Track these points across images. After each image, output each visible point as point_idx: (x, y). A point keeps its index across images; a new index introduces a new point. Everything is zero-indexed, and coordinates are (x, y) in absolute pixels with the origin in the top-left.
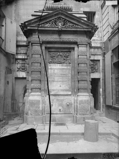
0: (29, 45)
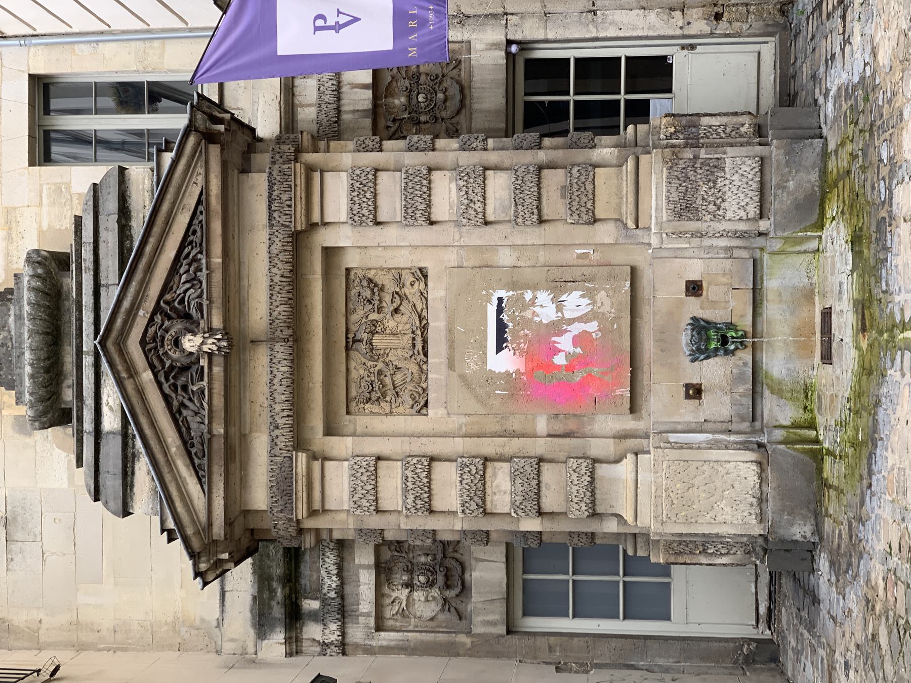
0: (318, 531)
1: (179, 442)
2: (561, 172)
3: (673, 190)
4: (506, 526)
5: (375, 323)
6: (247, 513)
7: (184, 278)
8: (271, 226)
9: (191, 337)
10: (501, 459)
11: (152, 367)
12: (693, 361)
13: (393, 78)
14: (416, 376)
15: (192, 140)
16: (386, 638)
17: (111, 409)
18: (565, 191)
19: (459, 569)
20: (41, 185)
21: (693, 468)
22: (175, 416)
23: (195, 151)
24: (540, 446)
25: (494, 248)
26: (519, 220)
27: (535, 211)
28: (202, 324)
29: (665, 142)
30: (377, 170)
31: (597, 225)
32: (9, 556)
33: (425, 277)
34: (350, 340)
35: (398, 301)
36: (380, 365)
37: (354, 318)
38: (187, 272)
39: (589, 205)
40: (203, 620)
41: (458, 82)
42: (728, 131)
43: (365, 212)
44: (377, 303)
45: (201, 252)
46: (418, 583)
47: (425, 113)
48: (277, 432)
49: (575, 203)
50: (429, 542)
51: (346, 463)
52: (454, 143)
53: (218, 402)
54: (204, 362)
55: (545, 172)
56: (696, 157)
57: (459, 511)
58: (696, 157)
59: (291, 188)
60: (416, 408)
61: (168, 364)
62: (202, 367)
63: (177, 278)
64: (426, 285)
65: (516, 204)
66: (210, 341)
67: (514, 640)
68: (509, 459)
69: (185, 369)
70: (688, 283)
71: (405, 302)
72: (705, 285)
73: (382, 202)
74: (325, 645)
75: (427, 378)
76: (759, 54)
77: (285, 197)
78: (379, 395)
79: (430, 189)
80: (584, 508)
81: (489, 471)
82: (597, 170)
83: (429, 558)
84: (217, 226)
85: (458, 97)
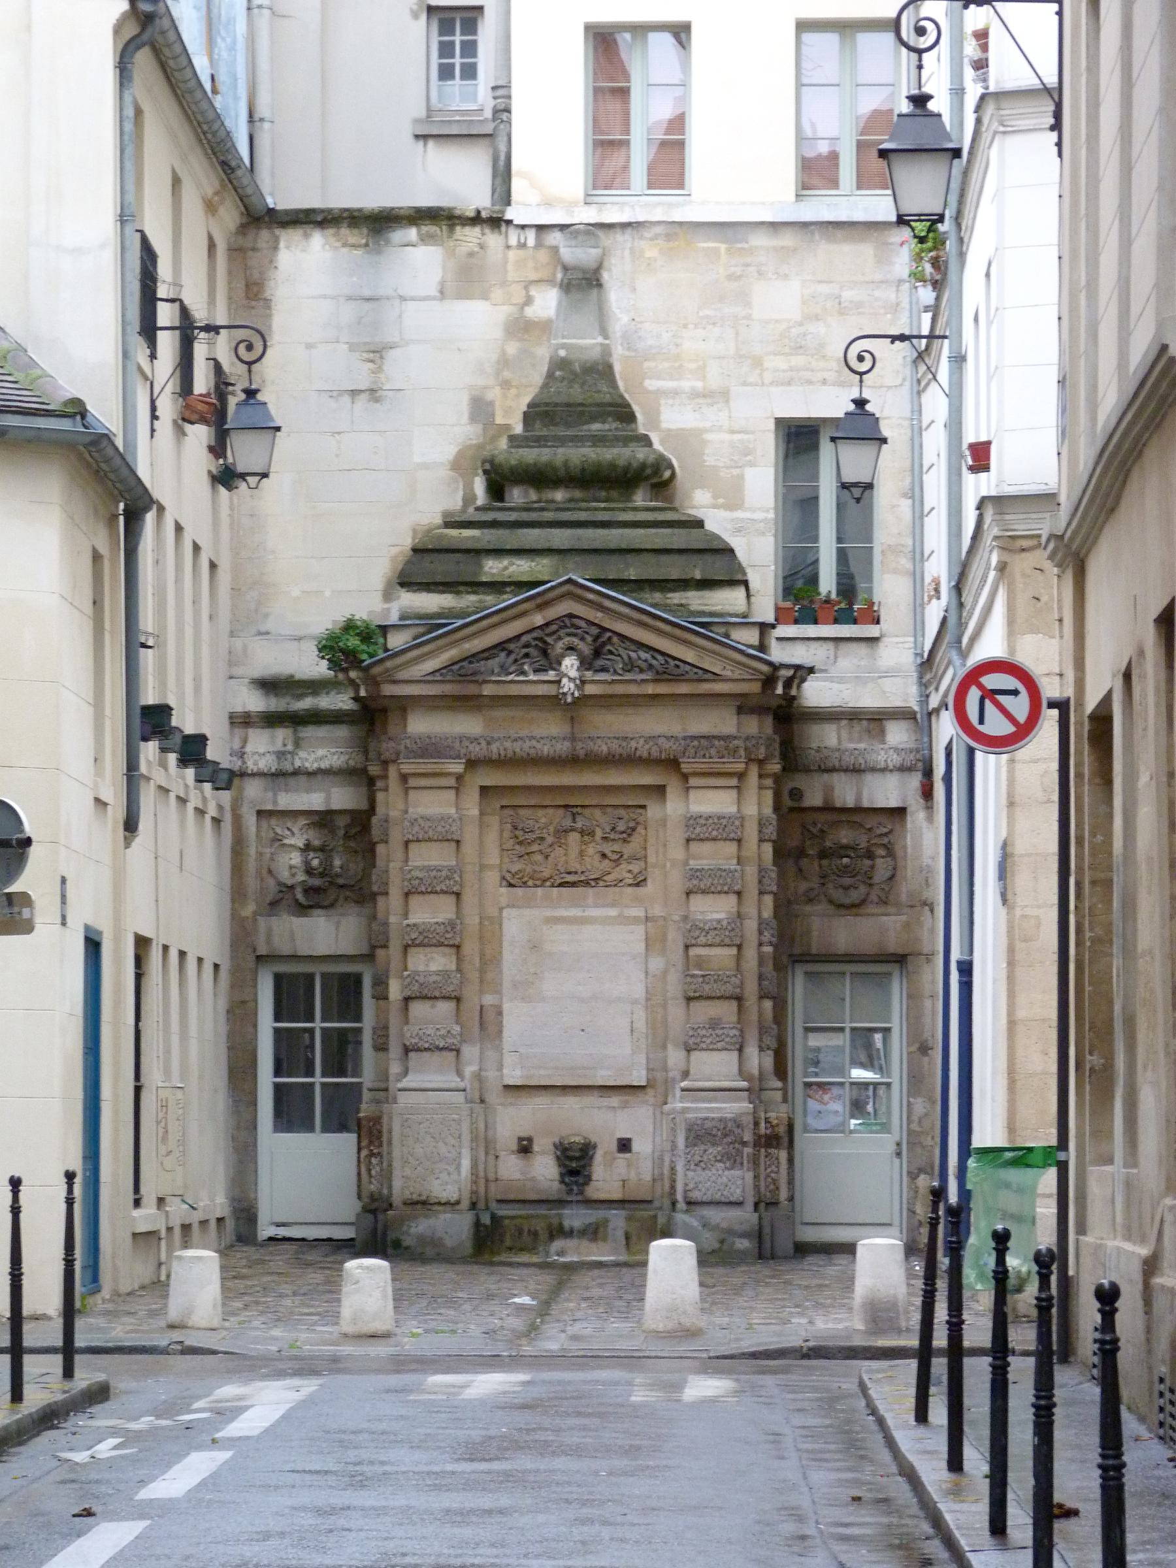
1: (475, 650)
2: (734, 1018)
3: (714, 1123)
4: (395, 965)
5: (592, 834)
6: (404, 710)
7: (633, 655)
8: (685, 738)
9: (575, 667)
10: (459, 960)
11: (547, 624)
12: (555, 1145)
13: (870, 830)
14: (537, 876)
15: (765, 668)
16: (250, 821)
17: (506, 568)
18: (714, 1024)
19: (326, 904)
20: (753, 433)
21: (453, 1142)
22: (501, 646)
23: (755, 669)
24: (472, 1001)
25: (663, 952)
26: (689, 979)
27: (697, 994)
28: (589, 675)
29: (762, 1115)
30: (739, 841)
31: (684, 1053)
32: (335, 394)
33: (637, 885)
34: (575, 810)
35: (615, 857)
36: (550, 840)
37: (597, 813)
38: (639, 658)
39: (704, 1046)
40: (266, 616)
41: (863, 902)
42: (773, 1175)
43: (698, 830)
44: (612, 836)
45: (657, 673)
46: (310, 857)
47: (830, 865)
48: (484, 743)
49: (704, 1032)
50: (375, 888)
51: (453, 811)
52: (768, 913)
53: (514, 690)
54: (551, 675)
55: (734, 1004)
56: (744, 1144)
57: (411, 921)
58: (744, 1144)
59: (723, 757)
60: (508, 876)
61: (549, 640)
62: (546, 670)
63: (633, 647)
64: (630, 885)
65: (703, 976)
66: (572, 686)
67: (250, 962)
68: (459, 970)
69: (545, 653)
70: (629, 1140)
71: (612, 864)
72: (627, 1155)
73: (707, 847)
74: (242, 755)
75: (536, 886)
76: (890, 1225)
77: (713, 751)
78: (521, 839)
79: (719, 893)
80: (413, 1041)
81: (447, 950)
82: (735, 1054)
83: (339, 870)
84: (684, 689)
85: (847, 901)
